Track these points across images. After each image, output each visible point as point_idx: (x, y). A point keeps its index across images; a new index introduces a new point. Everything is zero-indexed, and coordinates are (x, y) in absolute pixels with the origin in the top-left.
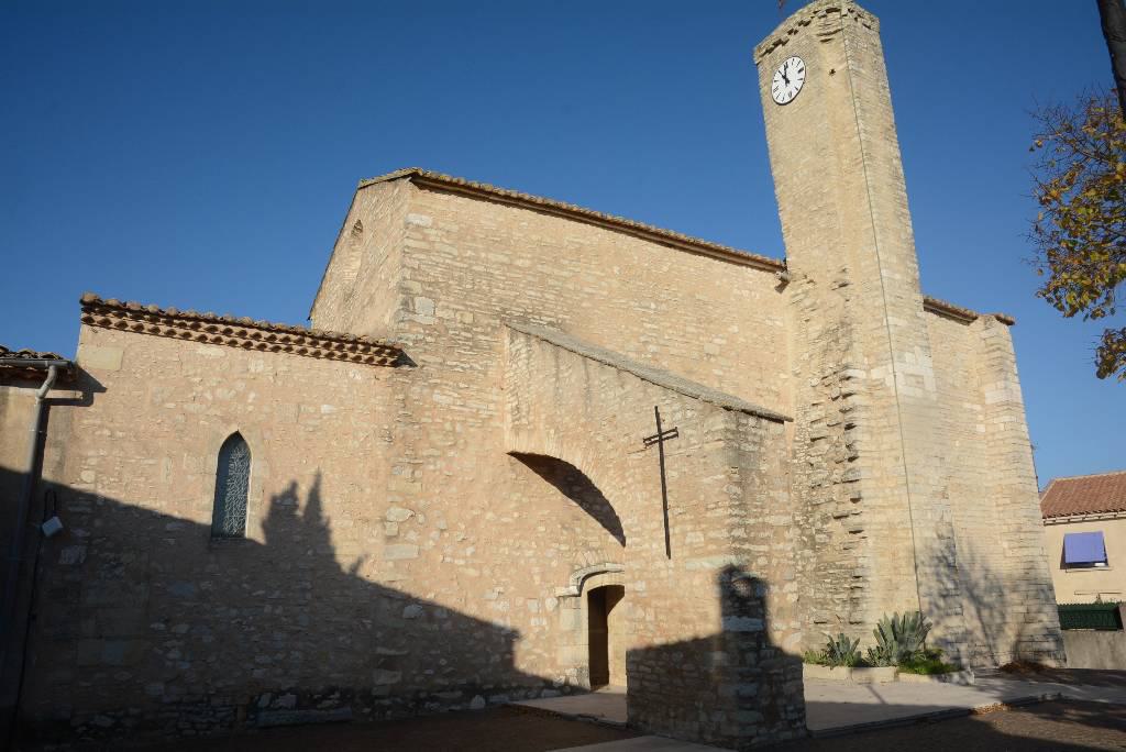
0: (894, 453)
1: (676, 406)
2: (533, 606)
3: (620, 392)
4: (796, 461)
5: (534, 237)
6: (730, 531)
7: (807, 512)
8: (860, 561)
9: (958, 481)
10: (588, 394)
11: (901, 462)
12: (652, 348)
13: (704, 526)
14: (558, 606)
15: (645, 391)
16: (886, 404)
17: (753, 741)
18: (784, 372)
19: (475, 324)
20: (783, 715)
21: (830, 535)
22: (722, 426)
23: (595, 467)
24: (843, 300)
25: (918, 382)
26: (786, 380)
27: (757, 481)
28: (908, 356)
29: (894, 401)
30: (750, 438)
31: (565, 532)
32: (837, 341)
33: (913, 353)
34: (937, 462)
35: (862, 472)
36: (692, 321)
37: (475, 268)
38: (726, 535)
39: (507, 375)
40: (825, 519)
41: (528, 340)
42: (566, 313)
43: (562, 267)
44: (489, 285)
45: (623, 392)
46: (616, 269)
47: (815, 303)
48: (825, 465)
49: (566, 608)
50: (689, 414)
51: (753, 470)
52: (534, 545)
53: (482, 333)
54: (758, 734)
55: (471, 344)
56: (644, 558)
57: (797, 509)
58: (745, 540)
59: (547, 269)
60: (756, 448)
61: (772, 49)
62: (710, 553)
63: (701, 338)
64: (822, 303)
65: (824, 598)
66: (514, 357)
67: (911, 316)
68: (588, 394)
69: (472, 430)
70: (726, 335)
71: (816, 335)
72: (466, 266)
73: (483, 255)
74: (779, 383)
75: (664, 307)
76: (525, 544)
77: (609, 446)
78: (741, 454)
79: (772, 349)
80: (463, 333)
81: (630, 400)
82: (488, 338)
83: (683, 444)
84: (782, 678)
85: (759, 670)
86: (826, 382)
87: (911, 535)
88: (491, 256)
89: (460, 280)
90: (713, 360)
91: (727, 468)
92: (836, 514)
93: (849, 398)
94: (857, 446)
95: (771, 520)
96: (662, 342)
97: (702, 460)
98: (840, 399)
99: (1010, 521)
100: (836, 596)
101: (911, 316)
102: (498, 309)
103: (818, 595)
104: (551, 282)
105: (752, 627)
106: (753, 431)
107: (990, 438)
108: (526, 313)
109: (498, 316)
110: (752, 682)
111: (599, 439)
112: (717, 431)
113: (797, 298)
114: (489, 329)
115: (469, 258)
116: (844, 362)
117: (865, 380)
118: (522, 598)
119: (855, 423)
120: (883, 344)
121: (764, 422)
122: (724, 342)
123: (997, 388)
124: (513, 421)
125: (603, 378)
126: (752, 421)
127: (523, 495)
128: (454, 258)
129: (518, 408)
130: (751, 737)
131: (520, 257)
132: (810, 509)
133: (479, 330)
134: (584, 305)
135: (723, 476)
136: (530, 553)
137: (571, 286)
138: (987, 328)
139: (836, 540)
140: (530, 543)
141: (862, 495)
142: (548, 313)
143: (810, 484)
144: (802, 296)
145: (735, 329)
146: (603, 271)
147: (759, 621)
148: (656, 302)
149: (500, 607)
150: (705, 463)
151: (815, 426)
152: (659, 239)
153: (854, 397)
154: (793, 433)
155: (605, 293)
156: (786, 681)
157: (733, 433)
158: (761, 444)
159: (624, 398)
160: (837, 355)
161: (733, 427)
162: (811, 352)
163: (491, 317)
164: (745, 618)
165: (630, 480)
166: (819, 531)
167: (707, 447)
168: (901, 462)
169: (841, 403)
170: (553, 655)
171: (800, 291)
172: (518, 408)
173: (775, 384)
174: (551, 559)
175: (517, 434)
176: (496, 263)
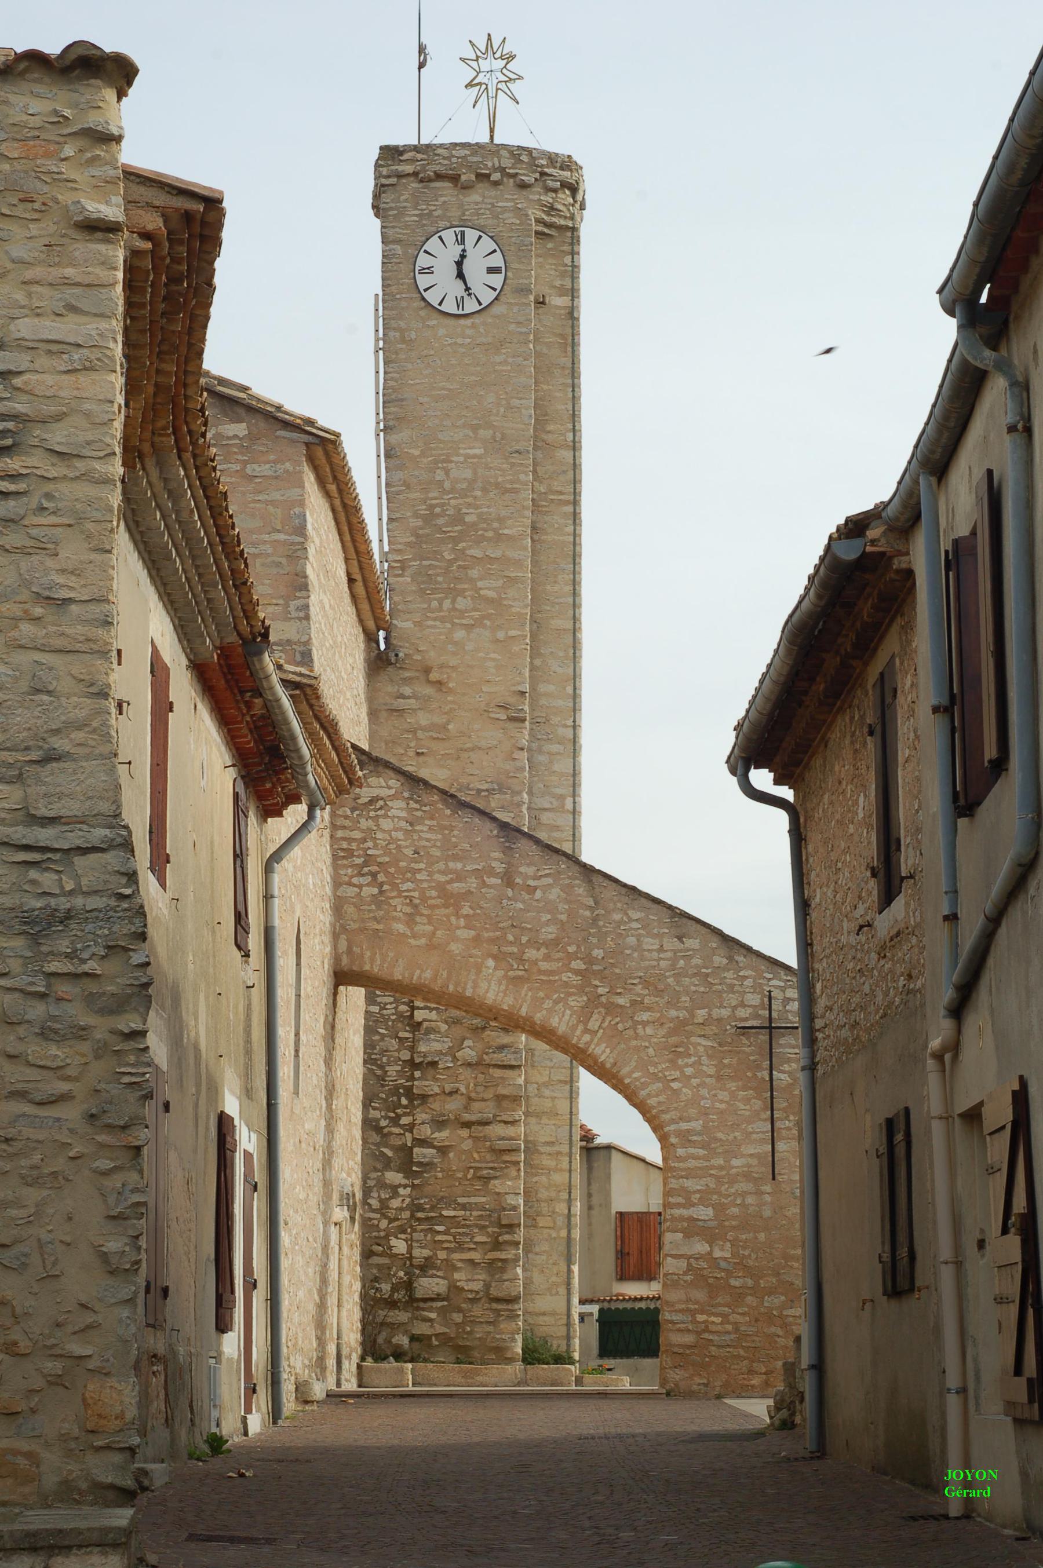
7: (400, 1106)
8: (511, 1200)
48: (444, 1027)
56: (711, 1175)
61: (430, 180)
87: (565, 1165)
100: (456, 1256)
113: (401, 703)
125: (635, 915)
132: (404, 1101)
171: (407, 691)
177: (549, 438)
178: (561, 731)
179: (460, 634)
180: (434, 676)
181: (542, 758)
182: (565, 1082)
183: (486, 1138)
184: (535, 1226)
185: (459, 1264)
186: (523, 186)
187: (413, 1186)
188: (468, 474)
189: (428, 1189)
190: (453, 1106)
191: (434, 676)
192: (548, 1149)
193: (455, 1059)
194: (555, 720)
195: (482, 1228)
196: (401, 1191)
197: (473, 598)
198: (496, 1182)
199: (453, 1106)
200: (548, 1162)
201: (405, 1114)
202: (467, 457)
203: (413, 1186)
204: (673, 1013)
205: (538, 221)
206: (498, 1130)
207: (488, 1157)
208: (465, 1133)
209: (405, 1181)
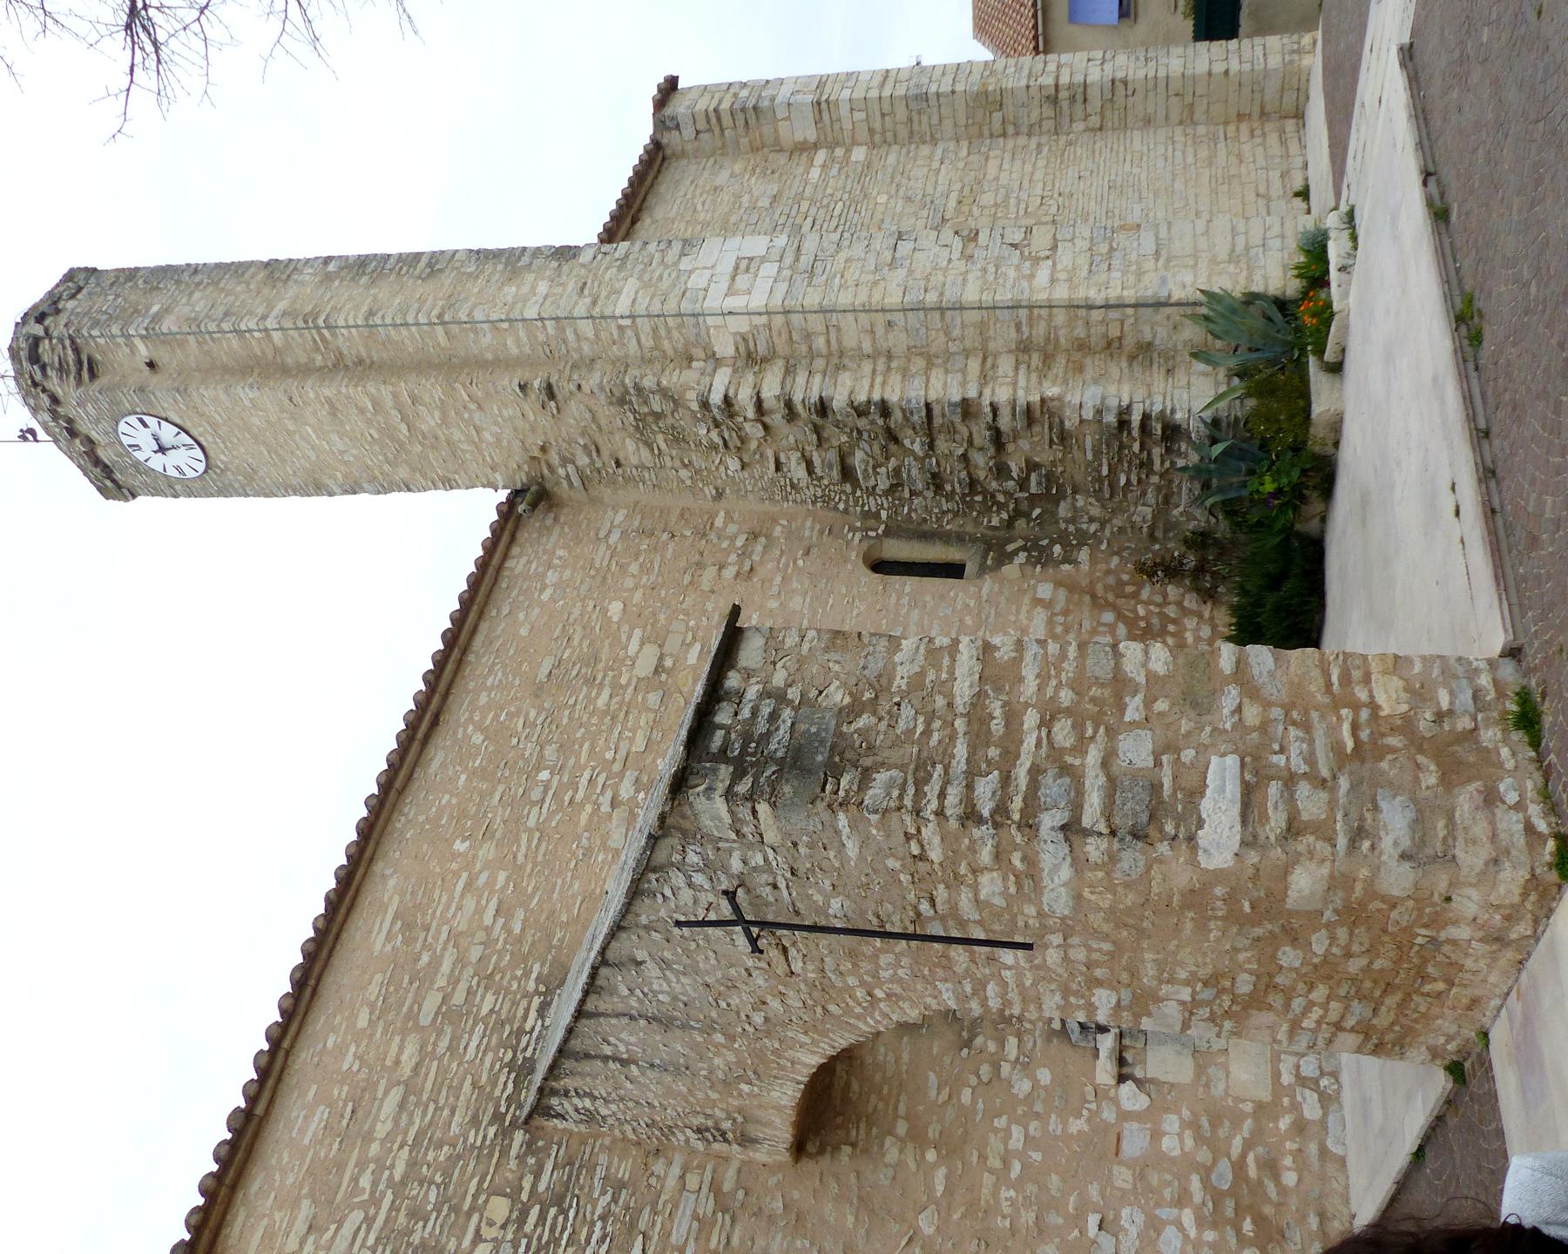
0: (880, 331)
1: (678, 879)
2: (1135, 1142)
3: (651, 969)
4: (884, 514)
5: (363, 1021)
6: (980, 821)
8: (1088, 414)
9: (952, 203)
10: (663, 1022)
11: (898, 318)
12: (626, 790)
13: (963, 869)
14: (1140, 1083)
15: (647, 928)
16: (785, 335)
17: (1542, 826)
18: (713, 516)
19: (514, 1196)
20: (1464, 723)
21: (1032, 466)
22: (720, 805)
23: (824, 1034)
24: (579, 395)
25: (747, 270)
26: (727, 513)
27: (864, 721)
28: (697, 281)
29: (778, 321)
30: (762, 727)
31: (979, 1041)
32: (658, 416)
33: (691, 272)
34: (905, 248)
35: (912, 394)
36: (587, 696)
37: (397, 1177)
38: (984, 831)
39: (631, 1136)
40: (1001, 471)
41: (554, 1092)
42: (527, 974)
43: (436, 963)
44: (439, 1146)
45: (650, 964)
46: (460, 846)
47: (585, 447)
48: (893, 463)
49: (1144, 1062)
50: (692, 858)
51: (839, 734)
52: (1000, 1123)
53: (537, 1176)
54: (1519, 806)
55: (553, 1211)
56: (1035, 984)
57: (976, 521)
58: (1006, 780)
59: (432, 1002)
60: (787, 713)
62: (1031, 861)
63: (623, 681)
64: (583, 434)
65: (1159, 488)
66: (590, 1117)
67: (620, 269)
68: (663, 1022)
69: (735, 1241)
70: (626, 628)
71: (645, 453)
72: (389, 1196)
73: (374, 1148)
74: (732, 529)
75: (550, 751)
76: (995, 1143)
77: (775, 1004)
78: (796, 761)
79: (665, 536)
80: (528, 1228)
81: (667, 955)
82: (549, 1166)
83: (765, 878)
84: (1364, 714)
85: (1344, 783)
86: (734, 441)
87: (1044, 312)
88: (381, 1130)
89: (417, 1214)
90: (668, 663)
91: (821, 806)
92: (992, 451)
93: (766, 405)
94: (862, 397)
95: (963, 691)
96: (617, 767)
97: (802, 850)
98: (766, 419)
99: (1035, 115)
100: (1157, 467)
101: (620, 269)
102: (492, 1131)
103: (1150, 497)
104: (459, 998)
105: (1229, 787)
106: (746, 713)
107: (877, 138)
108: (511, 1065)
109: (505, 1133)
110: (1376, 808)
111: (758, 1019)
112: (731, 812)
114: (531, 1161)
115: (375, 1184)
116: (695, 406)
117: (735, 371)
118: (1116, 1169)
119: (814, 397)
120: (669, 331)
121: (733, 680)
122: (638, 633)
123: (788, 118)
124: (726, 1140)
126: (723, 716)
127: (891, 1132)
128: (369, 1221)
129: (699, 1131)
130: (1529, 828)
131: (397, 1062)
132: (978, 498)
133: (527, 1184)
134: (517, 929)
135: (841, 816)
136: (1017, 1132)
137: (475, 953)
138: (678, 127)
139: (1044, 456)
140: (996, 1131)
141: (956, 398)
142: (520, 1013)
143: (930, 494)
144: (570, 468)
145: (615, 609)
146: (457, 874)
147: (1214, 760)
148: (538, 769)
149: (1133, 1231)
150: (811, 846)
151: (818, 471)
152: (415, 746)
153: (764, 395)
154: (831, 514)
155: (502, 876)
156: (1374, 706)
157: (737, 776)
158: (780, 697)
159: (665, 964)
160: (683, 420)
161: (725, 771)
162: (677, 463)
163: (505, 1152)
164: (1206, 806)
165: (852, 981)
166: (1023, 484)
167: (771, 836)
168: (898, 318)
169: (777, 419)
170: (1248, 1107)
172: (699, 1131)
173: (733, 539)
174: (1036, 1084)
175: (754, 1141)
176: (396, 1122)
177: (270, 353)
178: (551, 331)
179: (487, 436)
180: (537, 453)
181: (586, 348)
182: (943, 314)
183: (1014, 430)
184: (1120, 338)
185: (1167, 464)
186: (55, 400)
187: (1075, 492)
188: (335, 437)
189: (1079, 478)
190: (980, 460)
191: (537, 453)
192: (1025, 329)
193: (927, 456)
194: (541, 337)
195: (1121, 447)
196: (1080, 503)
197: (448, 428)
198: (1067, 424)
199: (980, 460)
200: (1040, 330)
201: (993, 496)
202: (318, 437)
203: (1075, 492)
204: (760, 982)
205: (79, 381)
206: (1004, 422)
207: (1036, 429)
208: (1010, 448)
209: (1069, 500)
